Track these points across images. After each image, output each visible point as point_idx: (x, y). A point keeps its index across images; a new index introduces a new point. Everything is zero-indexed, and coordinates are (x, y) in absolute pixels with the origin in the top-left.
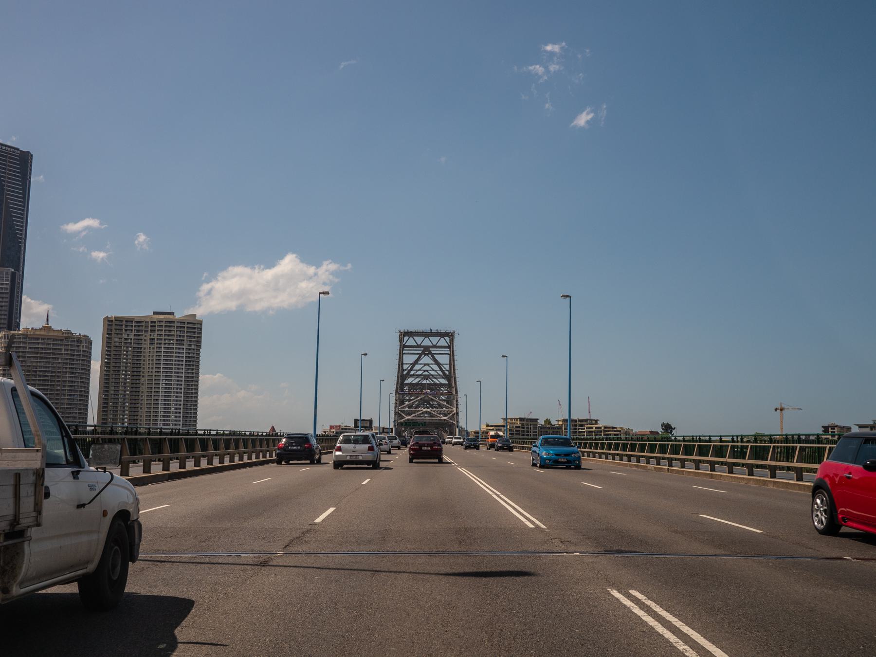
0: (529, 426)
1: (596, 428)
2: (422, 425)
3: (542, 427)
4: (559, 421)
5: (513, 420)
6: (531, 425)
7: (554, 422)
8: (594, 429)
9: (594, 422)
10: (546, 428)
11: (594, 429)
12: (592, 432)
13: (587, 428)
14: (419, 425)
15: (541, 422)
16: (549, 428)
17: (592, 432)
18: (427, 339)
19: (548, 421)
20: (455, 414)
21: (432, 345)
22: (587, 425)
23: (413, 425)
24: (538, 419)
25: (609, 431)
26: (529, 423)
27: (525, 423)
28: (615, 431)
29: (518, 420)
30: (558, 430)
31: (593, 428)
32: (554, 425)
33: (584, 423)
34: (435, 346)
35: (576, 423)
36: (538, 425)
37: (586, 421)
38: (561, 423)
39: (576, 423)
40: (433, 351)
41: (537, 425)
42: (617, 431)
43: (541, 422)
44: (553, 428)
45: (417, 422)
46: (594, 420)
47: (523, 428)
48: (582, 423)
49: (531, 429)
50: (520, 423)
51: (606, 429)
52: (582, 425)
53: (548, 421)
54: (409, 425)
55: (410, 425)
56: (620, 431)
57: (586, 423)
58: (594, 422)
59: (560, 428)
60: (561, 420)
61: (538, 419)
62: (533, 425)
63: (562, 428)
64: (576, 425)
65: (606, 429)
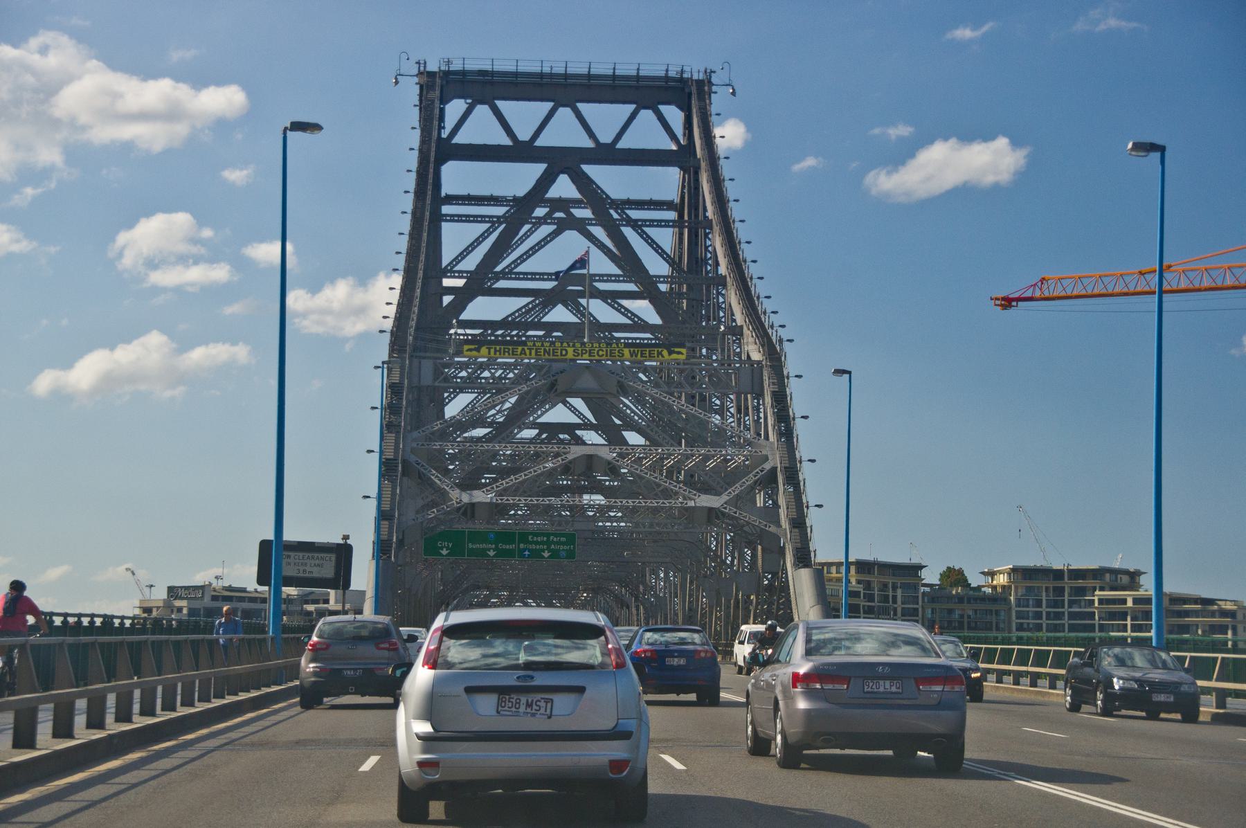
0: (891, 594)
1: (1136, 601)
2: (555, 554)
3: (936, 595)
4: (992, 574)
5: (834, 569)
6: (895, 588)
7: (975, 580)
8: (1130, 603)
9: (1125, 579)
10: (950, 598)
11: (1130, 603)
12: (1123, 616)
13: (1101, 601)
14: (536, 554)
15: (931, 576)
16: (960, 599)
17: (1123, 616)
18: (565, 113)
19: (954, 576)
20: (771, 477)
21: (590, 144)
22: (1102, 589)
23: (501, 554)
24: (921, 567)
25: (1187, 613)
26: (890, 581)
27: (875, 579)
28: (1213, 614)
29: (853, 569)
30: (994, 607)
31: (1124, 601)
32: (979, 588)
33: (1089, 583)
34: (609, 154)
35: (1058, 584)
36: (922, 589)
37: (1098, 573)
38: (1002, 580)
39: (1058, 584)
40: (604, 176)
41: (915, 587)
42: (1224, 613)
43: (931, 576)
44: (976, 599)
45: (524, 537)
46: (1126, 572)
47: (870, 598)
48: (1080, 583)
49: (895, 601)
50: (859, 582)
51: (1177, 608)
52: (1081, 591)
53: (954, 576)
54: (472, 552)
55: (483, 553)
56: (1232, 614)
57: (1097, 583)
58: (1125, 579)
59: (999, 598)
60: (1000, 572)
61: (921, 567)
62: (904, 586)
63: (1006, 601)
64: (1060, 590)
65: (1177, 608)
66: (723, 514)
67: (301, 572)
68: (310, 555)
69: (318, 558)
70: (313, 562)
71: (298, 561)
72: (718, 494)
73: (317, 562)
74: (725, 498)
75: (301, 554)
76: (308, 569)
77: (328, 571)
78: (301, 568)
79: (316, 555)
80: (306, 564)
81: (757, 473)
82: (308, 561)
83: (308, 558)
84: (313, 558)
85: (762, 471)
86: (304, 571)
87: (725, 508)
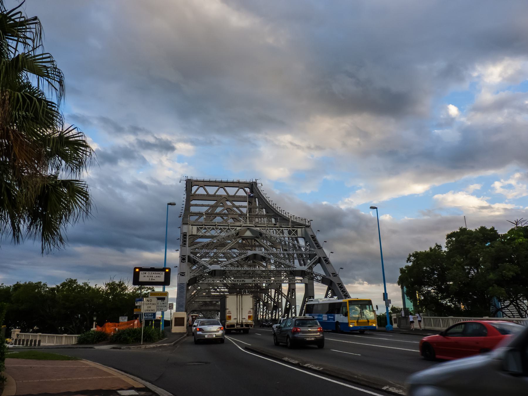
67: (151, 279)
68: (154, 272)
69: (157, 273)
70: (156, 275)
71: (149, 275)
73: (157, 275)
75: (151, 272)
76: (153, 278)
77: (162, 279)
78: (151, 278)
79: (156, 272)
80: (152, 277)
82: (154, 275)
83: (153, 273)
84: (155, 273)
86: (152, 279)
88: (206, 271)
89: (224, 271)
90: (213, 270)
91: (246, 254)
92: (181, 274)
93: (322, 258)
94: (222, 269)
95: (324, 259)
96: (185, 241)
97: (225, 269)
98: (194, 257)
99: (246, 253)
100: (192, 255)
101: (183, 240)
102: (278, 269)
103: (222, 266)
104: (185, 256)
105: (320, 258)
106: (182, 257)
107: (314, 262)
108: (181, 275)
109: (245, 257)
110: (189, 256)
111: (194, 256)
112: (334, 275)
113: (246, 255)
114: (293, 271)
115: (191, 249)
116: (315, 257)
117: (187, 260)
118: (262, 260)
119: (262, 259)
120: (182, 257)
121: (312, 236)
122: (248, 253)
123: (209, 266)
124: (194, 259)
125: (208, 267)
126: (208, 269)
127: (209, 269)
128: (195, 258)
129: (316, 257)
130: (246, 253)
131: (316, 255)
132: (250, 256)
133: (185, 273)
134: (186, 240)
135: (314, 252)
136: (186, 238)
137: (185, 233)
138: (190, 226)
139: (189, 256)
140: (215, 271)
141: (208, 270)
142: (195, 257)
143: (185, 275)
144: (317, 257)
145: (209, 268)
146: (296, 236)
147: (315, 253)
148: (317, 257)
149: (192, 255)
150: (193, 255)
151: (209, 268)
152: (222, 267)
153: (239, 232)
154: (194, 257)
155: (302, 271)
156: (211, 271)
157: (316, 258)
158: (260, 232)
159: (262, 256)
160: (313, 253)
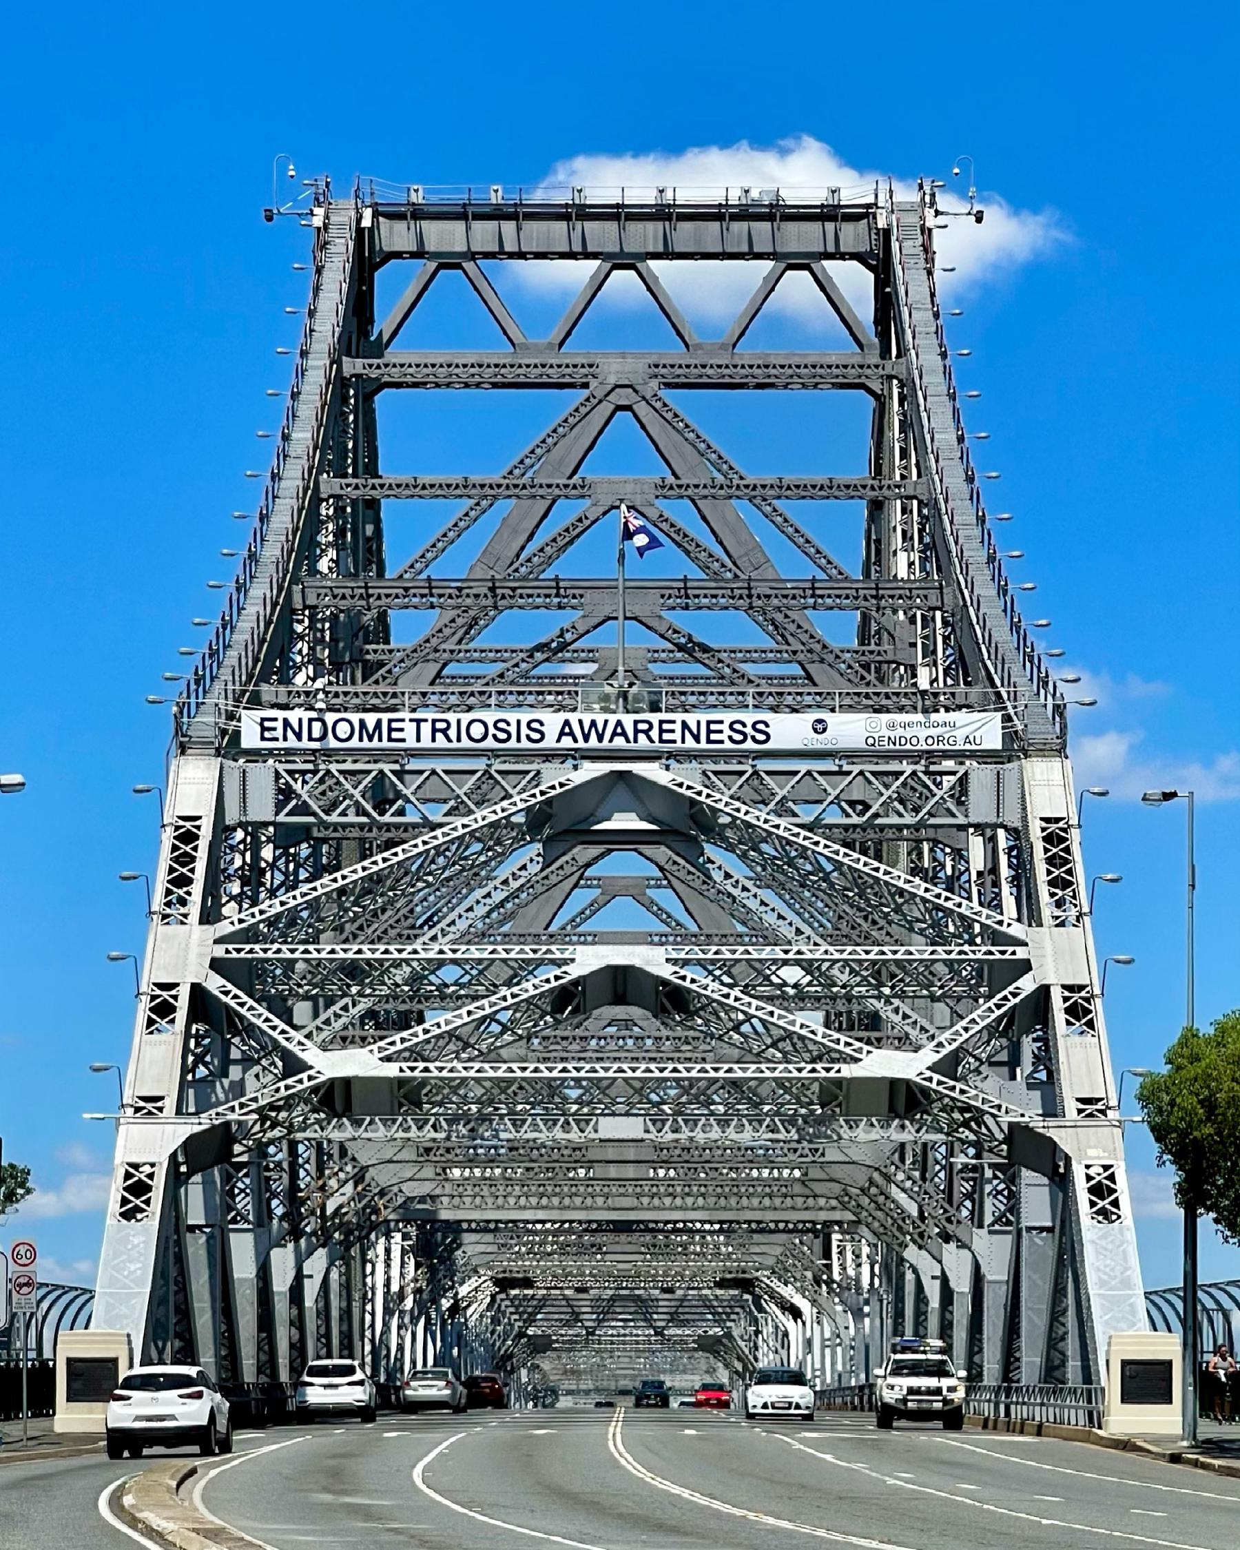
66: (925, 1092)
72: (903, 1042)
74: (928, 1056)
81: (1005, 998)
85: (1015, 995)
87: (930, 1079)
88: (287, 1088)
89: (401, 1082)
90: (332, 1082)
91: (558, 972)
92: (142, 1104)
93: (1057, 996)
94: (391, 1070)
95: (1066, 999)
96: (183, 881)
97: (408, 1073)
98: (226, 993)
99: (566, 962)
100: (214, 983)
101: (172, 870)
102: (740, 1074)
103: (393, 1049)
104: (177, 985)
105: (1044, 991)
106: (153, 998)
107: (999, 1020)
108: (138, 1110)
109: (552, 990)
110: (198, 992)
111: (230, 987)
112: (1090, 1108)
113: (557, 978)
114: (839, 1083)
115: (216, 942)
116: (1011, 988)
117: (181, 1015)
118: (662, 1004)
119: (665, 1000)
120: (153, 998)
121: (1053, 827)
122: (573, 960)
123: (310, 1054)
124: (226, 1006)
125: (305, 1063)
126: (304, 1076)
127: (312, 1072)
128: (232, 1003)
129: (1018, 983)
130: (566, 962)
131: (1025, 966)
132: (584, 977)
133: (161, 1098)
134: (192, 871)
135: (1018, 949)
136: (193, 859)
137: (188, 825)
138: (229, 763)
139: (198, 992)
140: (347, 1083)
141: (300, 1081)
142: (235, 997)
143: (160, 1109)
144: (1027, 984)
145: (311, 1068)
146: (961, 820)
147: (1021, 953)
148: (1027, 984)
149: (214, 983)
150: (224, 982)
151: (311, 1068)
152: (388, 1059)
153: (549, 802)
154: (226, 993)
155: (894, 1083)
156: (324, 1083)
157: (1015, 995)
158: (693, 802)
159: (665, 983)
160: (1006, 956)
